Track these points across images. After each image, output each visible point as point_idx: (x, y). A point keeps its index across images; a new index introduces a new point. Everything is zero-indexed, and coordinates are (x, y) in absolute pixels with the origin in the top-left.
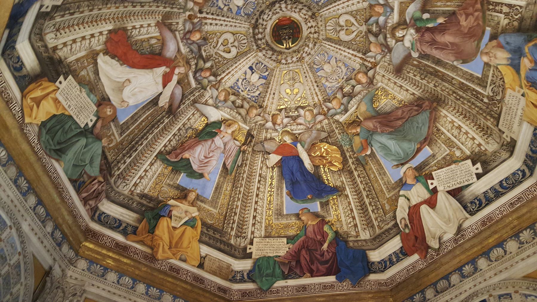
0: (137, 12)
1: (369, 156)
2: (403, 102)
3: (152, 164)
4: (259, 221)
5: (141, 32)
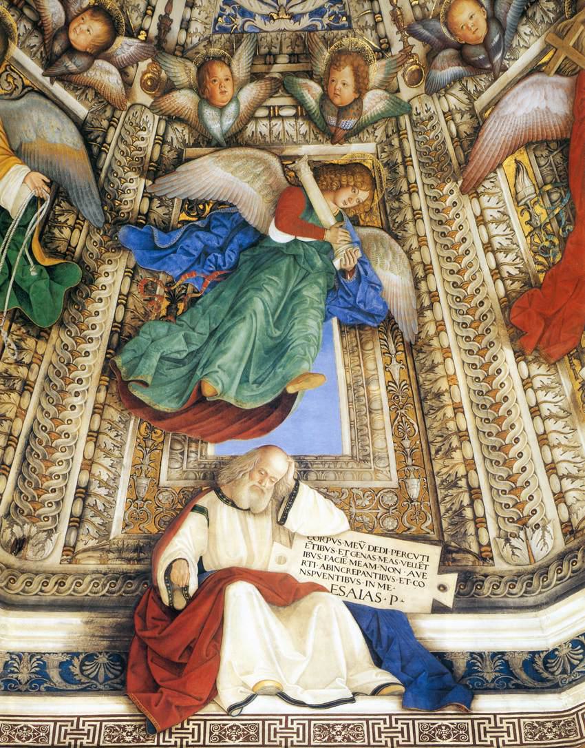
5: (505, 243)
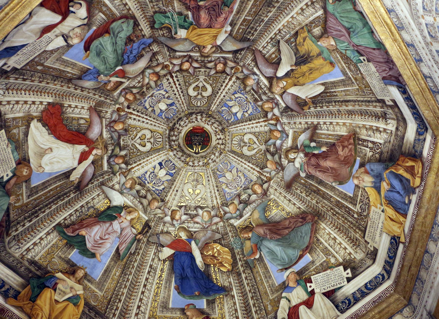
0: (76, 95)
1: (258, 260)
2: (290, 214)
3: (48, 234)
4: (143, 311)
5: (74, 111)
